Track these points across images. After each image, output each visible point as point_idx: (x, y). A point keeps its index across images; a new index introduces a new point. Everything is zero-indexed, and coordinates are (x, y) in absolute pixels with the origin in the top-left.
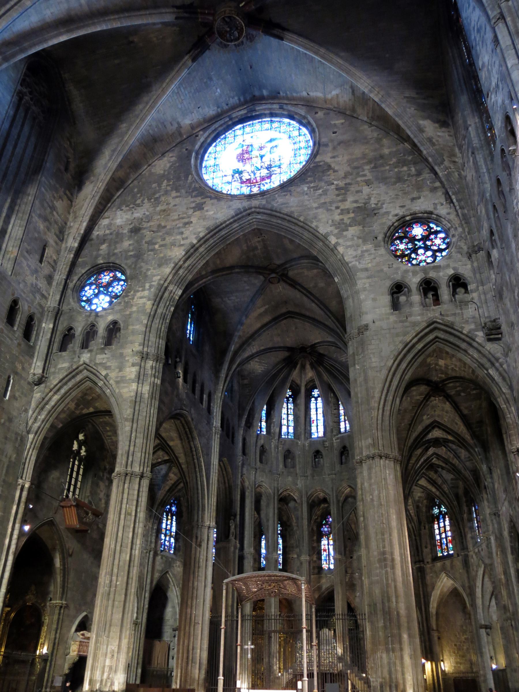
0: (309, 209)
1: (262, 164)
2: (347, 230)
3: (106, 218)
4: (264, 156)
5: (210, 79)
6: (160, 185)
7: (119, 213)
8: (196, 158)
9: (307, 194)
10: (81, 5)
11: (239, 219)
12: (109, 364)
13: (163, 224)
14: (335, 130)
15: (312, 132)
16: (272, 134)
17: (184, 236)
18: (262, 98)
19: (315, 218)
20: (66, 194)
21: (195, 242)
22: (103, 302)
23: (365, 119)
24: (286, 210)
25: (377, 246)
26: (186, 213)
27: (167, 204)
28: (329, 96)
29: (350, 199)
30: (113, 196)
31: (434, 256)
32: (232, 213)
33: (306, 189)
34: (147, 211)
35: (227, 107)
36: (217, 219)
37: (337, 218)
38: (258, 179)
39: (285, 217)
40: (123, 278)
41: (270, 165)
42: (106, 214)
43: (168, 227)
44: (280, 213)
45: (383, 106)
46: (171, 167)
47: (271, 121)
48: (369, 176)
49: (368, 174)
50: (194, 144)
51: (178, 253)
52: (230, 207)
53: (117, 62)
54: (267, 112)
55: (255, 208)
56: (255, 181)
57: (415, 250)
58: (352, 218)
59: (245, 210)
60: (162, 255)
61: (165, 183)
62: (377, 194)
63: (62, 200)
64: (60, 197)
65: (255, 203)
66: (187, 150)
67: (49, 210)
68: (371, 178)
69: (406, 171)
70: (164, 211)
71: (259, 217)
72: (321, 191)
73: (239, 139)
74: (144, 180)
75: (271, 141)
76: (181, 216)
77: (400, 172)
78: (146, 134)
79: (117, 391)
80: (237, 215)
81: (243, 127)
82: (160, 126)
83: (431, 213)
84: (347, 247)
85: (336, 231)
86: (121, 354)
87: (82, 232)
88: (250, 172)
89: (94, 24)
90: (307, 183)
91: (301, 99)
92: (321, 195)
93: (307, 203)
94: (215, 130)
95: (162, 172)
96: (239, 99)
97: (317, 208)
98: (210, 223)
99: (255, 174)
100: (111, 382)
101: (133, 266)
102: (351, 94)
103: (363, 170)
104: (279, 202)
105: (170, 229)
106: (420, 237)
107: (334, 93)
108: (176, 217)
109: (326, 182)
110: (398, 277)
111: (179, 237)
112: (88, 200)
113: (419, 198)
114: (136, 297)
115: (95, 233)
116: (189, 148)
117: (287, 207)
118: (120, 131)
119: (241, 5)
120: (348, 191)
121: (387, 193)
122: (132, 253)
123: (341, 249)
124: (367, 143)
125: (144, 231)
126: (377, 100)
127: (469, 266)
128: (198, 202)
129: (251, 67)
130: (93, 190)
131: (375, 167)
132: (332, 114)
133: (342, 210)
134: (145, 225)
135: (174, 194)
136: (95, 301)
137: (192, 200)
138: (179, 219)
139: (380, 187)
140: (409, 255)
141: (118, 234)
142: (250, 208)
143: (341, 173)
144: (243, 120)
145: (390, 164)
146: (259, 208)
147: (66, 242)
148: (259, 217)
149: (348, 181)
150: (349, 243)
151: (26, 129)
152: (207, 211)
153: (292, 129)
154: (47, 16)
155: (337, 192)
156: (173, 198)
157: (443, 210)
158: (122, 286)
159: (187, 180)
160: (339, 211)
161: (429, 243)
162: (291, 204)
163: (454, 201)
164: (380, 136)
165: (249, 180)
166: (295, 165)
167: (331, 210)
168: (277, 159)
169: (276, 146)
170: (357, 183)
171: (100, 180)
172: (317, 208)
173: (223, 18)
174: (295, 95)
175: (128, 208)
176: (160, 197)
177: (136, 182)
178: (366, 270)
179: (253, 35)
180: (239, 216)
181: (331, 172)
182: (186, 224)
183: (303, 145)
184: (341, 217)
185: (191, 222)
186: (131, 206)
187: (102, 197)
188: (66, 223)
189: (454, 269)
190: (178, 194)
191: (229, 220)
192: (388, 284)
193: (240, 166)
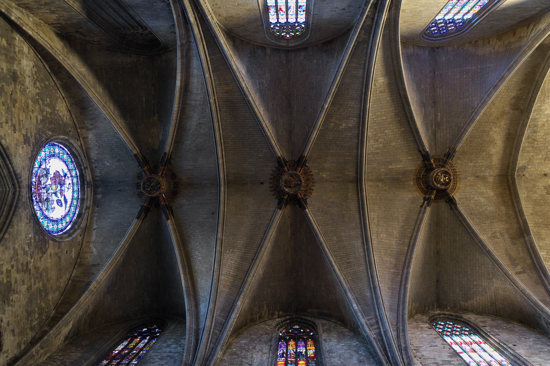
0: (14, 240)
3: (29, 51)
4: (56, 196)
5: (118, 161)
6: (48, 105)
7: (31, 64)
8: (63, 139)
9: (26, 237)
10: (191, 100)
11: (11, 176)
13: (17, 105)
14: (68, 252)
17: (4, 124)
18: (95, 193)
19: (6, 248)
20: (59, 23)
23: (73, 275)
24: (15, 220)
26: (23, 128)
27: (33, 110)
28: (92, 245)
29: (18, 276)
30: (46, 62)
32: (18, 171)
33: (30, 236)
34: (30, 91)
35: (94, 167)
36: (15, 156)
39: (9, 220)
41: (49, 201)
42: (32, 51)
44: (13, 215)
45: (86, 292)
46: (60, 116)
48: (34, 288)
49: (36, 286)
50: (73, 137)
52: (24, 169)
53: (144, 99)
55: (20, 192)
56: (39, 188)
58: (3, 282)
59: (18, 182)
61: (50, 111)
62: (20, 299)
63: (54, 20)
64: (58, 19)
65: (24, 191)
66: (70, 131)
67: (53, 9)
68: (33, 290)
69: (35, 317)
70: (28, 107)
71: (10, 194)
72: (27, 249)
74: (54, 91)
76: (21, 122)
77: (34, 313)
78: (90, 104)
80: (16, 175)
81: (77, 177)
82: (92, 116)
87: (24, 28)
88: (47, 184)
89: (179, 103)
90: (34, 236)
91: (91, 223)
92: (24, 250)
93: (19, 239)
94: (80, 156)
96: (97, 176)
97: (14, 248)
98: (12, 150)
99: (44, 188)
102: (93, 263)
103: (39, 282)
104: (23, 213)
105: (12, 112)
107: (94, 250)
108: (21, 118)
109: (33, 252)
112: (50, 42)
115: (18, 37)
116: (71, 133)
117: (18, 221)
118: (97, 85)
119: (163, 195)
120: (25, 273)
121: (20, 307)
124: (57, 280)
125: (13, 86)
126: (91, 287)
128: (31, 139)
129: (120, 190)
130: (57, 49)
131: (40, 291)
132: (79, 247)
133: (10, 271)
134: (18, 87)
135: (40, 118)
137: (33, 134)
138: (19, 121)
139: (25, 299)
141: (13, 59)
142: (20, 187)
143: (38, 264)
144: (82, 177)
145: (41, 302)
146: (19, 195)
147: (16, 9)
148: (10, 194)
149: (32, 271)
151: (121, 20)
152: (23, 148)
153: (71, 216)
154: (194, 79)
155: (25, 263)
156: (37, 116)
159: (49, 130)
160: (10, 268)
162: (19, 224)
164: (61, 289)
165: (40, 182)
166: (47, 221)
167: (11, 261)
168: (53, 206)
169: (62, 204)
170: (30, 279)
171: (65, 58)
172: (14, 248)
173: (160, 184)
174: (95, 219)
175: (34, 73)
176: (39, 104)
177: (53, 84)
179: (142, 197)
180: (14, 177)
181: (40, 255)
182: (14, 126)
183: (60, 226)
184: (5, 271)
185: (15, 132)
187: (48, 53)
188: (33, 14)
190: (39, 122)
191: (12, 167)
193: (51, 175)
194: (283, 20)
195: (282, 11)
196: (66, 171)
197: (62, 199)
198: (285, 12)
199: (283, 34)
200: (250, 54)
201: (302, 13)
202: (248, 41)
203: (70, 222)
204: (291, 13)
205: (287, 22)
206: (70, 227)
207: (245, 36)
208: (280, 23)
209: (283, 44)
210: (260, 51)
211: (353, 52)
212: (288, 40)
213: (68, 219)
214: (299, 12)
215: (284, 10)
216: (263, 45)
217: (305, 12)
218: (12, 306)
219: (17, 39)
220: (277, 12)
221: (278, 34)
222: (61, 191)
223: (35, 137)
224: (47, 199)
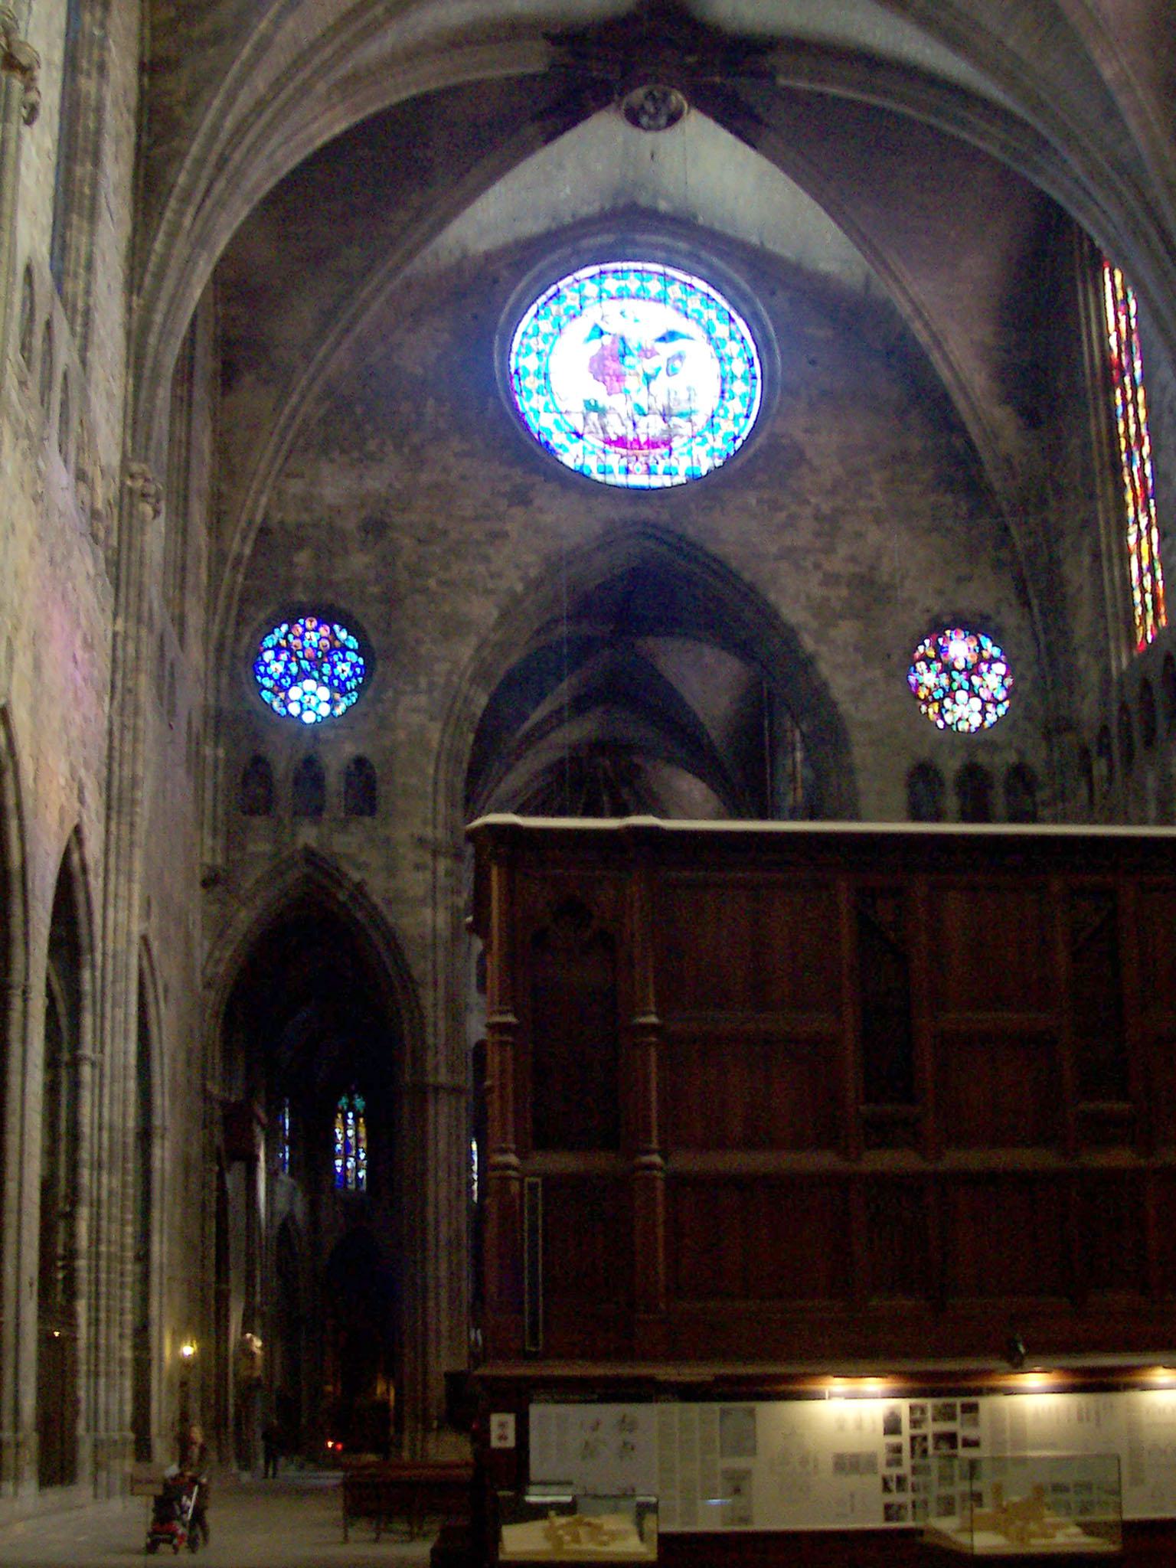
1: (651, 399)
2: (836, 626)
4: (654, 377)
7: (327, 470)
12: (363, 858)
15: (763, 346)
16: (666, 318)
17: (493, 568)
21: (519, 588)
22: (314, 700)
24: (713, 548)
25: (890, 676)
29: (843, 550)
31: (983, 712)
32: (598, 528)
33: (754, 502)
37: (818, 592)
38: (643, 439)
40: (353, 643)
43: (454, 535)
47: (664, 275)
49: (879, 496)
51: (483, 611)
54: (661, 254)
57: (950, 693)
60: (447, 608)
65: (646, 512)
66: (475, 317)
70: (437, 486)
73: (592, 314)
75: (669, 337)
79: (391, 920)
80: (607, 533)
81: (602, 272)
83: (988, 618)
84: (837, 667)
85: (814, 624)
86: (388, 840)
88: (624, 416)
95: (419, 371)
97: (779, 557)
100: (377, 899)
101: (383, 626)
106: (960, 665)
108: (469, 513)
110: (924, 753)
111: (481, 568)
113: (970, 578)
114: (401, 708)
122: (375, 590)
123: (824, 668)
127: (1043, 753)
134: (398, 519)
135: (456, 444)
136: (295, 693)
137: (503, 470)
140: (941, 701)
146: (654, 526)
150: (840, 659)
152: (541, 510)
157: (1011, 619)
158: (353, 666)
161: (975, 680)
163: (1036, 610)
165: (621, 442)
168: (683, 396)
169: (680, 357)
178: (868, 725)
181: (805, 469)
183: (739, 367)
185: (505, 535)
186: (356, 454)
189: (1020, 753)
190: (466, 447)
192: (906, 764)
193: (597, 392)
196: (582, 327)
197: (667, 350)
203: (732, 320)
206: (740, 322)
213: (722, 330)
218: (903, 578)
219: (279, 516)
222: (646, 353)
223: (511, 464)
224: (665, 416)
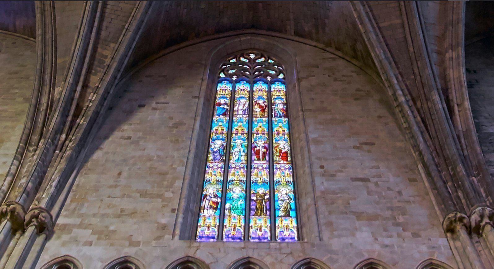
194: (260, 86)
195: (260, 106)
198: (254, 103)
199: (262, 59)
200: (325, 23)
201: (222, 101)
202: (328, 49)
204: (243, 101)
205: (252, 82)
207: (334, 59)
208: (266, 82)
209: (261, 41)
210: (306, 29)
211: (126, 22)
212: (252, 49)
214: (228, 102)
215: (257, 109)
216: (301, 40)
217: (217, 101)
220: (270, 104)
221: (270, 61)
